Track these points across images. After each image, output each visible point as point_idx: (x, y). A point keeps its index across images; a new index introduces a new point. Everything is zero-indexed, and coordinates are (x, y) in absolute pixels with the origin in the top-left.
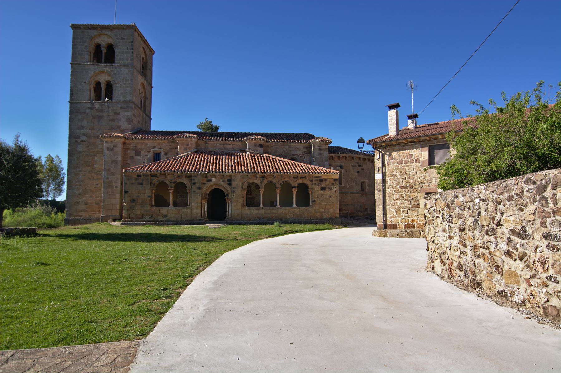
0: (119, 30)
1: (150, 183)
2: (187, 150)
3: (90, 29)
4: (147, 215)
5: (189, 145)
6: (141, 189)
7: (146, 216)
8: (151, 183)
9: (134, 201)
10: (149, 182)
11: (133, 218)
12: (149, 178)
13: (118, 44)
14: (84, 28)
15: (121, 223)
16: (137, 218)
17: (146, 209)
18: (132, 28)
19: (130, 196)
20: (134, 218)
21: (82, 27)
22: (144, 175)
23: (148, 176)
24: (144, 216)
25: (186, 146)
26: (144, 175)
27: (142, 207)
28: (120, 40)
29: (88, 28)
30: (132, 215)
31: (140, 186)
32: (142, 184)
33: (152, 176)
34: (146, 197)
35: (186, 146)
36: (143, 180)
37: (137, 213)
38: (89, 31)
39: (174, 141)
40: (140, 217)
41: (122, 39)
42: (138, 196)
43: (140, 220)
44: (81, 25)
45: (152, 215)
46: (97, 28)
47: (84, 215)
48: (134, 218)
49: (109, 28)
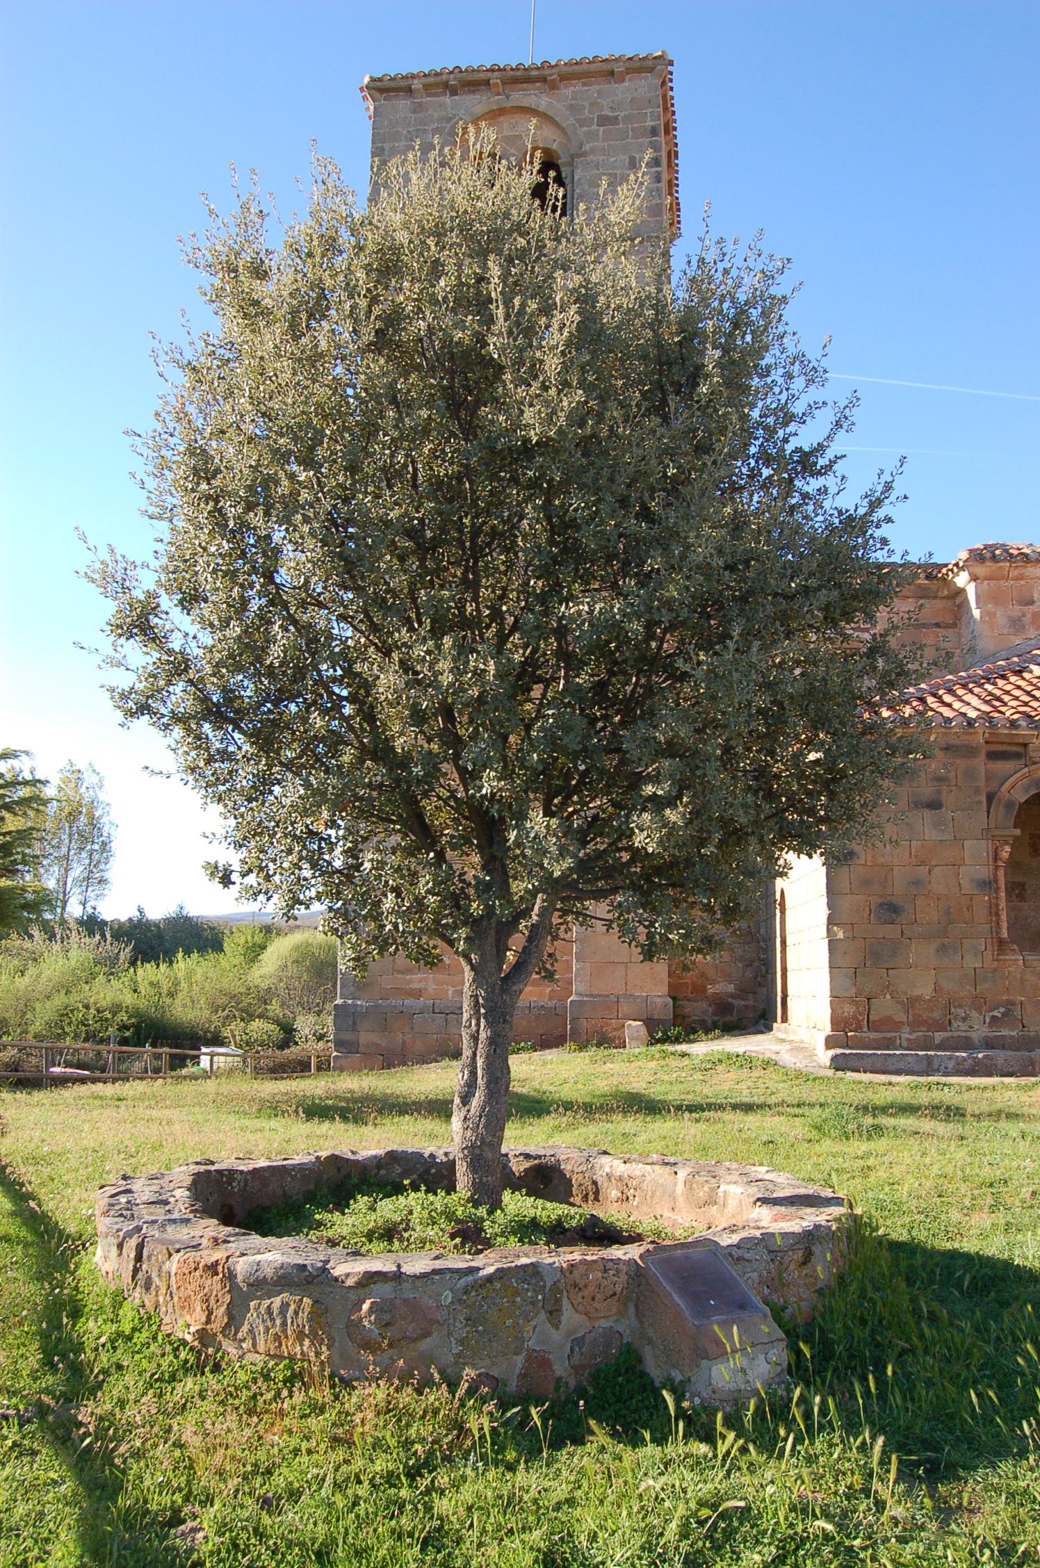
0: (584, 84)
1: (984, 799)
2: (1024, 627)
3: (454, 92)
4: (979, 1002)
5: (1032, 602)
6: (931, 835)
7: (974, 1014)
8: (990, 798)
9: (890, 910)
10: (977, 791)
11: (887, 1024)
12: (980, 764)
13: (587, 147)
14: (427, 87)
15: (834, 1059)
16: (916, 1024)
17: (972, 962)
18: (651, 70)
19: (866, 883)
20: (897, 1026)
21: (417, 85)
22: (947, 749)
23: (970, 752)
24: (961, 1013)
25: (1016, 610)
26: (947, 749)
27: (942, 950)
28: (594, 127)
29: (446, 85)
30: (885, 1006)
31: (927, 813)
32: (934, 805)
33: (993, 756)
34: (967, 887)
35: (1016, 610)
36: (939, 779)
37: (917, 992)
38: (447, 99)
39: (933, 585)
40: (936, 1014)
41: (603, 121)
42: (917, 883)
43: (939, 1036)
44: (413, 76)
45: (1011, 1003)
46: (487, 83)
47: (432, 987)
48: (897, 1026)
49: (544, 80)
